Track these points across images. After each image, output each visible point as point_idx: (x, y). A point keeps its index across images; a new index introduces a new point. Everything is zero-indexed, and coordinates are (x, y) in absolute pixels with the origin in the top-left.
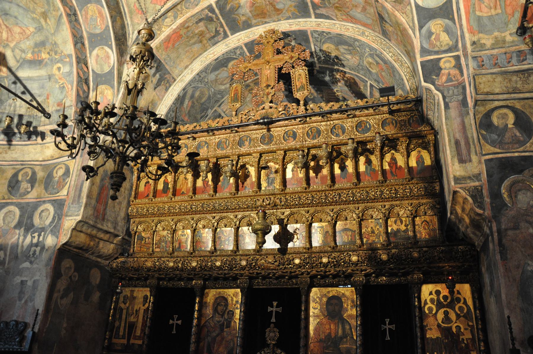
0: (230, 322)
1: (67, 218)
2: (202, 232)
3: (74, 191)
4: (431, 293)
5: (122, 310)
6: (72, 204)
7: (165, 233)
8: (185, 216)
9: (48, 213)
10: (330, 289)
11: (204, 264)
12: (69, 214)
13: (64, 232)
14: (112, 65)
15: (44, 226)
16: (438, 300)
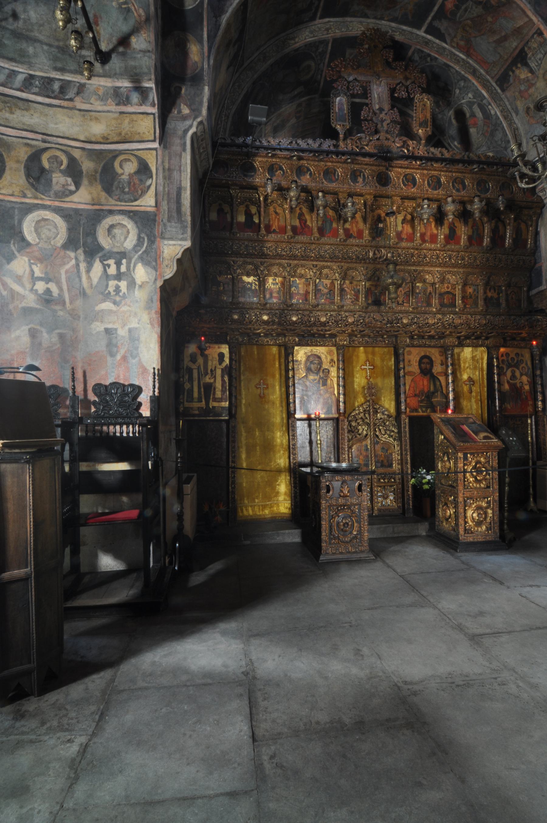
0: (326, 380)
1: (166, 242)
2: (298, 281)
3: (166, 202)
4: (502, 356)
5: (190, 371)
6: (169, 221)
7: (251, 279)
8: (280, 261)
9: (125, 230)
10: (421, 349)
11: (306, 319)
12: (166, 236)
13: (166, 262)
15: (123, 250)
16: (508, 361)
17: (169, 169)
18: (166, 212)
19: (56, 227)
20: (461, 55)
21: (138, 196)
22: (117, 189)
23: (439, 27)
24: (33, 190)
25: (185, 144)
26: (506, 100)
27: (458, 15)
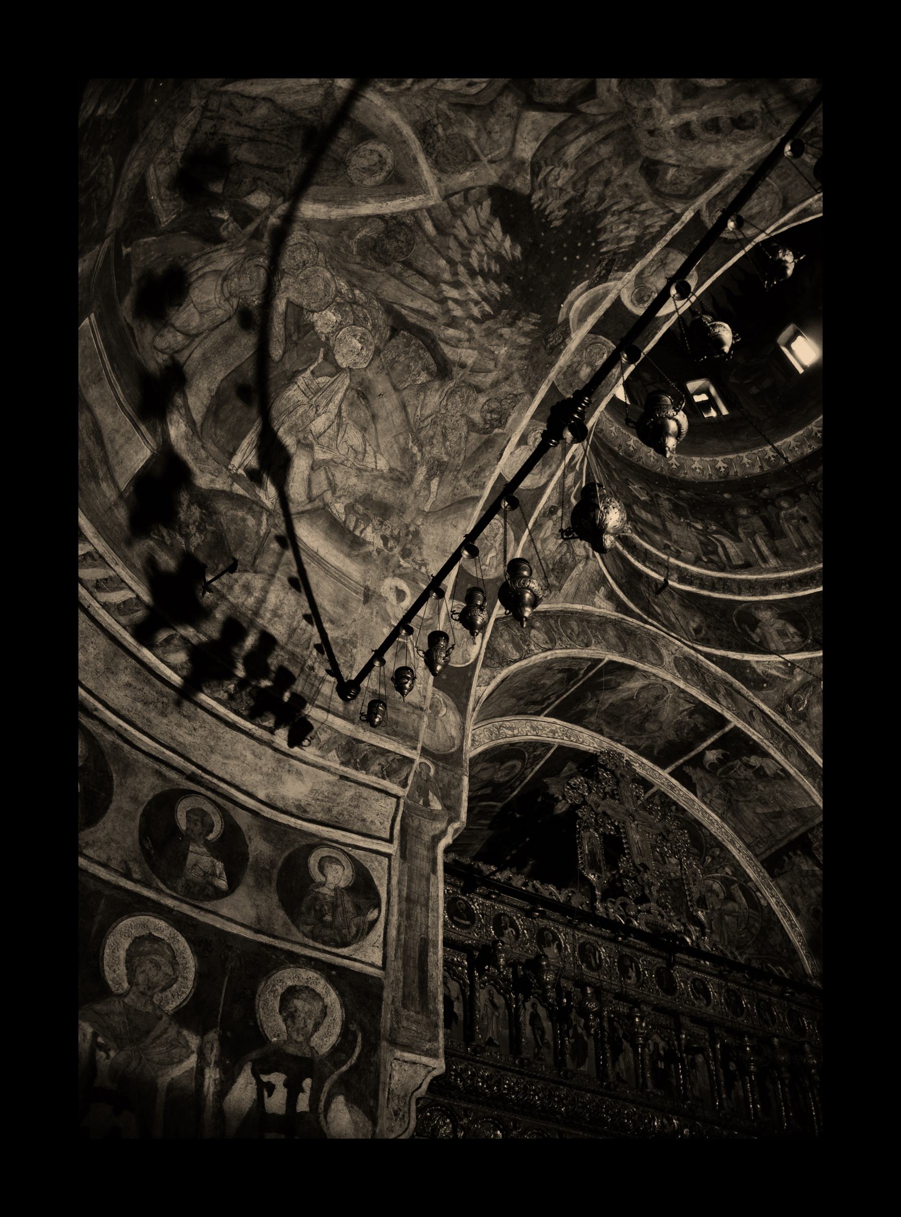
1: (398, 1054)
3: (400, 963)
6: (405, 1006)
9: (317, 1007)
12: (401, 1040)
17: (408, 899)
18: (402, 984)
19: (173, 962)
20: (713, 815)
21: (349, 938)
22: (309, 909)
23: (691, 774)
24: (146, 866)
25: (434, 861)
26: (776, 891)
27: (720, 770)
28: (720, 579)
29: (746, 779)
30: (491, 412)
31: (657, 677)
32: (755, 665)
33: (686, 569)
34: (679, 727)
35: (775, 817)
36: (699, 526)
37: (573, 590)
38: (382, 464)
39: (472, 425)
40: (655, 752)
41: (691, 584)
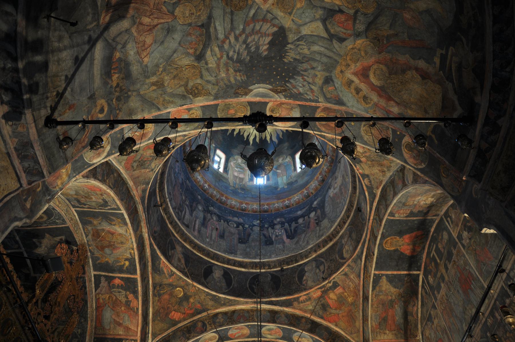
14: (91, 163)
23: (102, 282)
27: (115, 290)
28: (176, 222)
29: (120, 301)
30: (197, 88)
31: (130, 235)
32: (161, 262)
33: (169, 208)
34: (117, 261)
35: (117, 324)
36: (184, 198)
37: (136, 176)
38: (146, 60)
39: (186, 85)
40: (98, 262)
41: (166, 214)
